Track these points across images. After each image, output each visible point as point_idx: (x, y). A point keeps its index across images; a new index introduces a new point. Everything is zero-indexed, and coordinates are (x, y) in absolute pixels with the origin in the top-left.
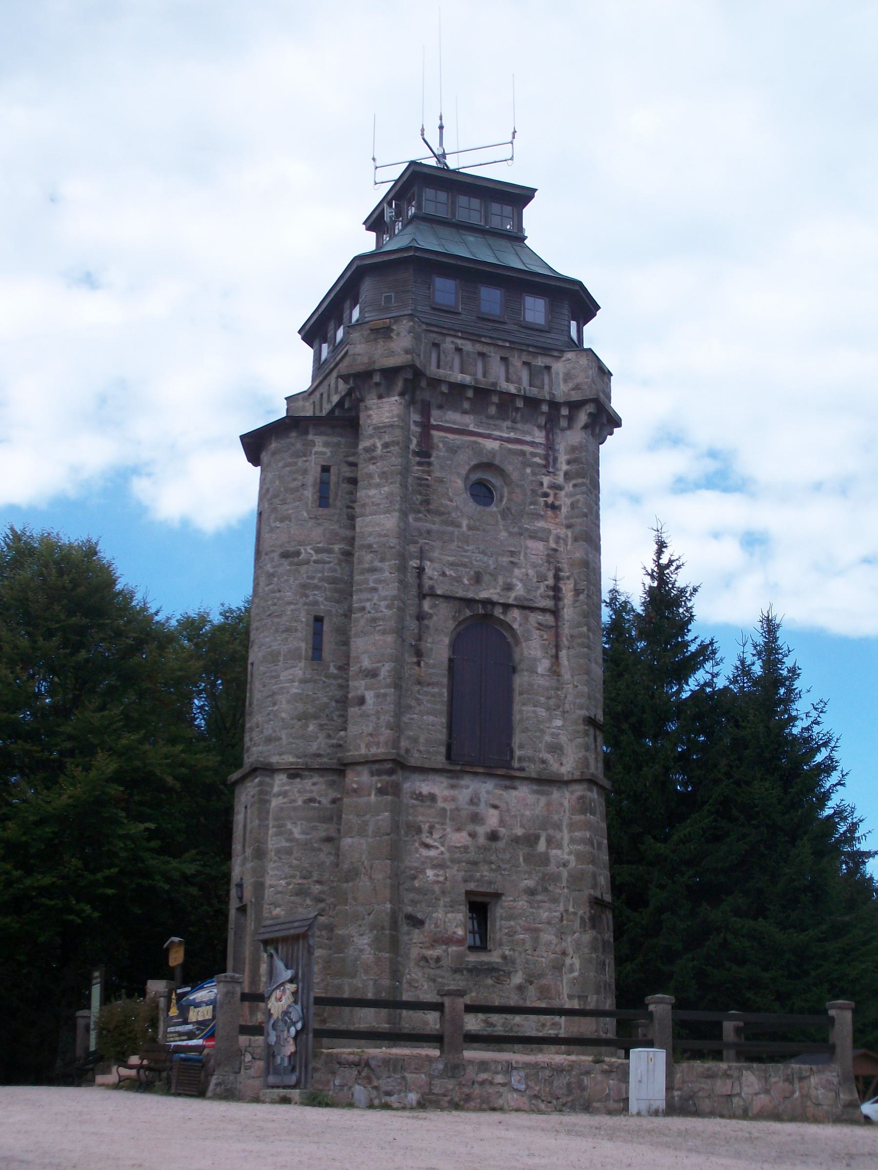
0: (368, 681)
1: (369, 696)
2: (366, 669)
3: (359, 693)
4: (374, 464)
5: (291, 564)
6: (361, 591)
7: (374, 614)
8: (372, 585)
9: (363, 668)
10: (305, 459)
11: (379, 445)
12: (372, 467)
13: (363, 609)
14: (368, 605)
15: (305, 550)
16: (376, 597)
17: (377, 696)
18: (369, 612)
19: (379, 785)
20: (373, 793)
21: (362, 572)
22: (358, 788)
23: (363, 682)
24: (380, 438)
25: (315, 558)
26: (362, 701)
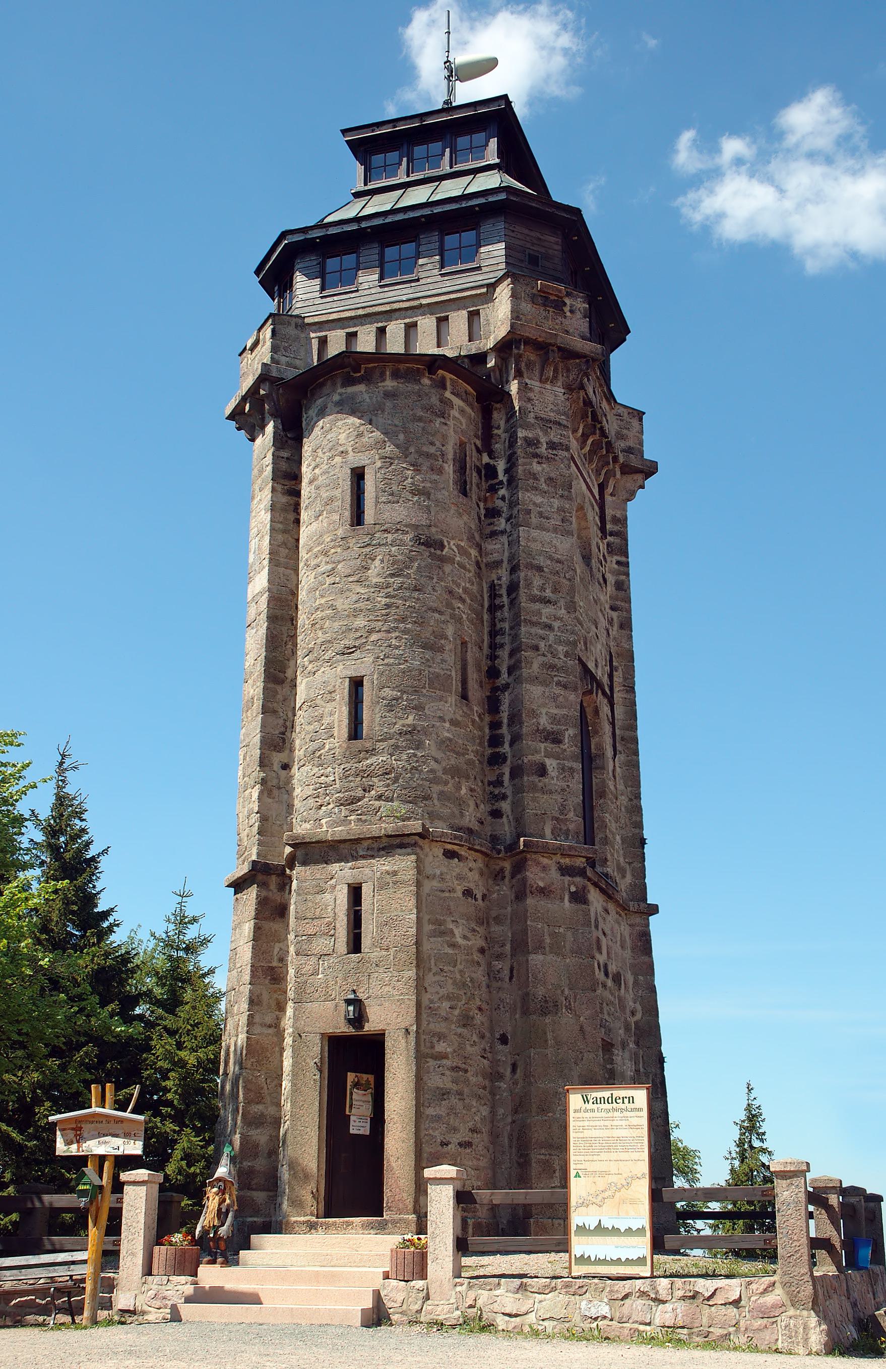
0: (549, 746)
1: (551, 764)
2: (544, 729)
3: (537, 758)
4: (539, 463)
5: (431, 555)
6: (534, 624)
7: (549, 659)
8: (544, 619)
9: (541, 728)
10: (443, 420)
11: (543, 440)
12: (536, 467)
13: (536, 648)
14: (542, 645)
15: (449, 544)
16: (552, 638)
17: (563, 769)
18: (544, 655)
19: (573, 889)
20: (567, 898)
21: (534, 599)
22: (544, 888)
23: (542, 745)
24: (546, 433)
25: (458, 559)
26: (542, 771)
